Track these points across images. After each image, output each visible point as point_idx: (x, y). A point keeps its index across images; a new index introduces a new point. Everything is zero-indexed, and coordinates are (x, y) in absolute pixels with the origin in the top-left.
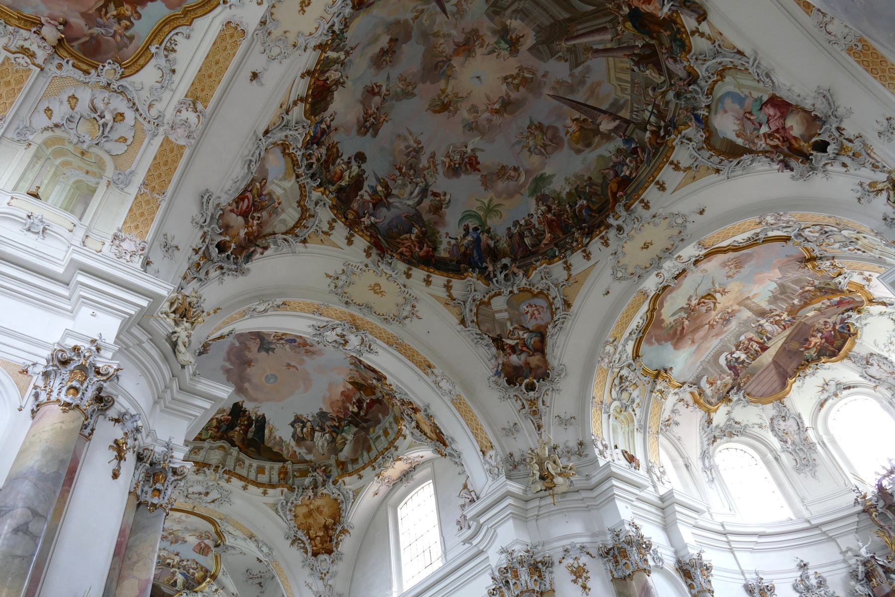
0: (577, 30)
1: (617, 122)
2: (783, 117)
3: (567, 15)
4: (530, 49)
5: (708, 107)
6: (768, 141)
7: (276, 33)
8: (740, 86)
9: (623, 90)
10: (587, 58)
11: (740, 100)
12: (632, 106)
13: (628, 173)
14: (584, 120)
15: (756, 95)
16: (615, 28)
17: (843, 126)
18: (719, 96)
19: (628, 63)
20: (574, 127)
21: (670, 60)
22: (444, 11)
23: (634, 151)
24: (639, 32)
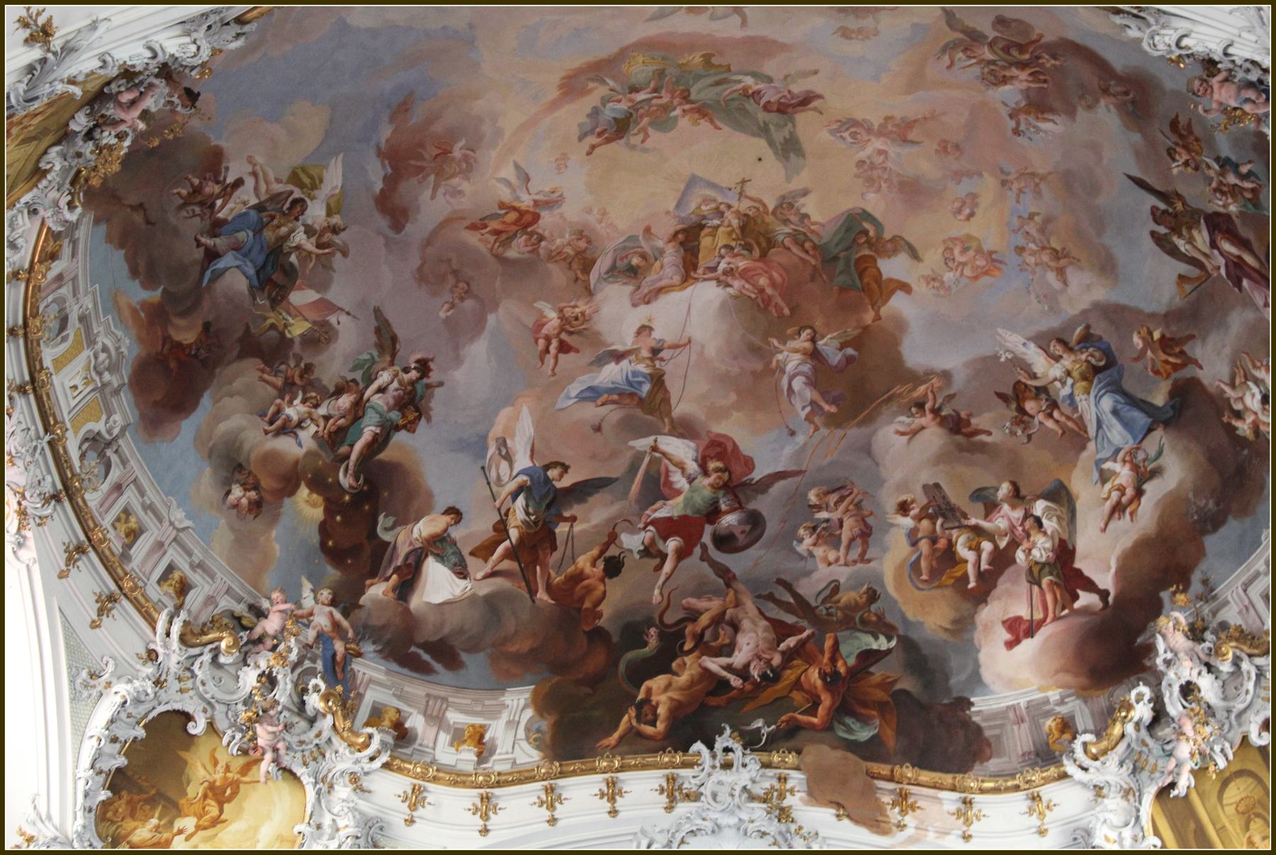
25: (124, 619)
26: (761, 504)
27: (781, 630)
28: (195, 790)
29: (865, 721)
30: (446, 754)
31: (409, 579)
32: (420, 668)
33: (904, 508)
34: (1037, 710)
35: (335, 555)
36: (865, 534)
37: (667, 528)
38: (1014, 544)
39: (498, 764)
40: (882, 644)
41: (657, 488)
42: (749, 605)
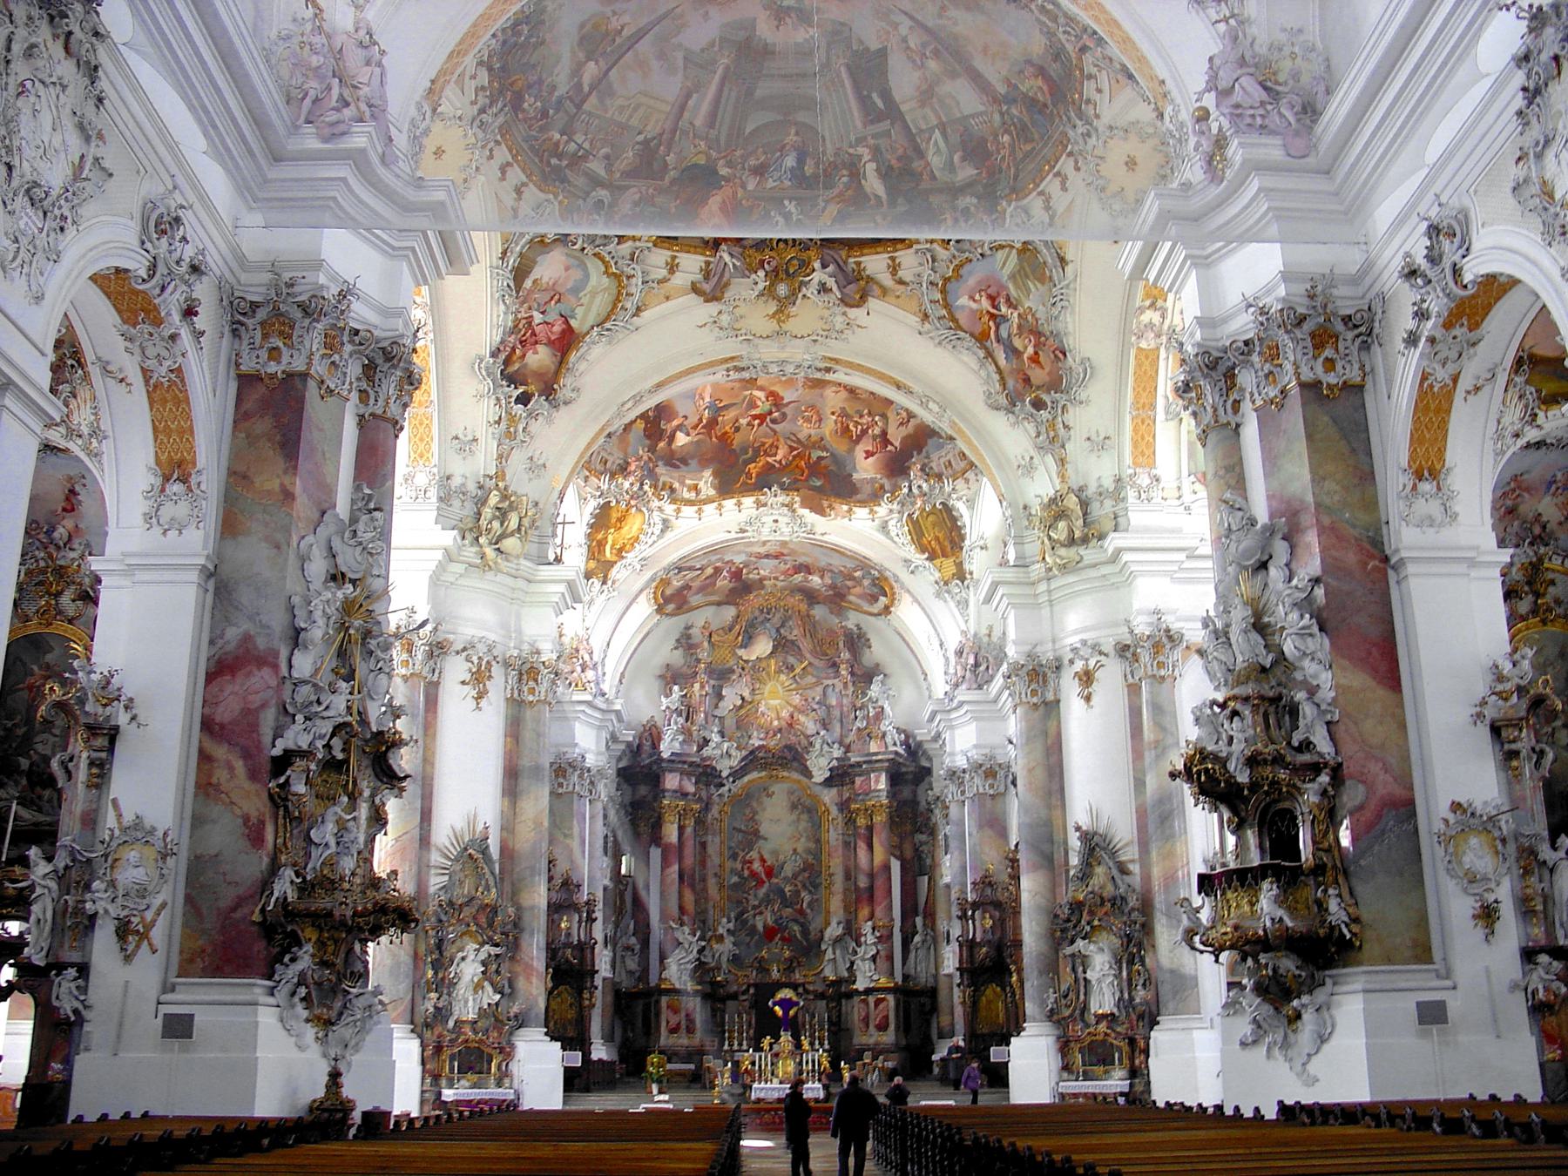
0: (730, 90)
1: (586, 89)
2: (550, 343)
3: (759, 93)
4: (751, 25)
5: (584, 249)
6: (524, 321)
7: (1156, 141)
8: (594, 294)
9: (622, 108)
10: (686, 78)
11: (576, 290)
12: (598, 117)
13: (526, 105)
14: (614, 40)
15: (579, 311)
16: (706, 139)
17: (540, 418)
18: (589, 265)
19: (652, 130)
20: (615, 24)
21: (637, 197)
22: (906, 13)
23: (545, 114)
24: (688, 168)
25: (593, 480)
26: (785, 410)
27: (792, 449)
28: (613, 521)
29: (819, 479)
30: (686, 495)
31: (672, 438)
32: (678, 467)
33: (833, 413)
34: (873, 480)
35: (648, 437)
36: (820, 420)
37: (755, 417)
38: (868, 428)
39: (702, 496)
40: (825, 454)
41: (752, 404)
42: (782, 440)
